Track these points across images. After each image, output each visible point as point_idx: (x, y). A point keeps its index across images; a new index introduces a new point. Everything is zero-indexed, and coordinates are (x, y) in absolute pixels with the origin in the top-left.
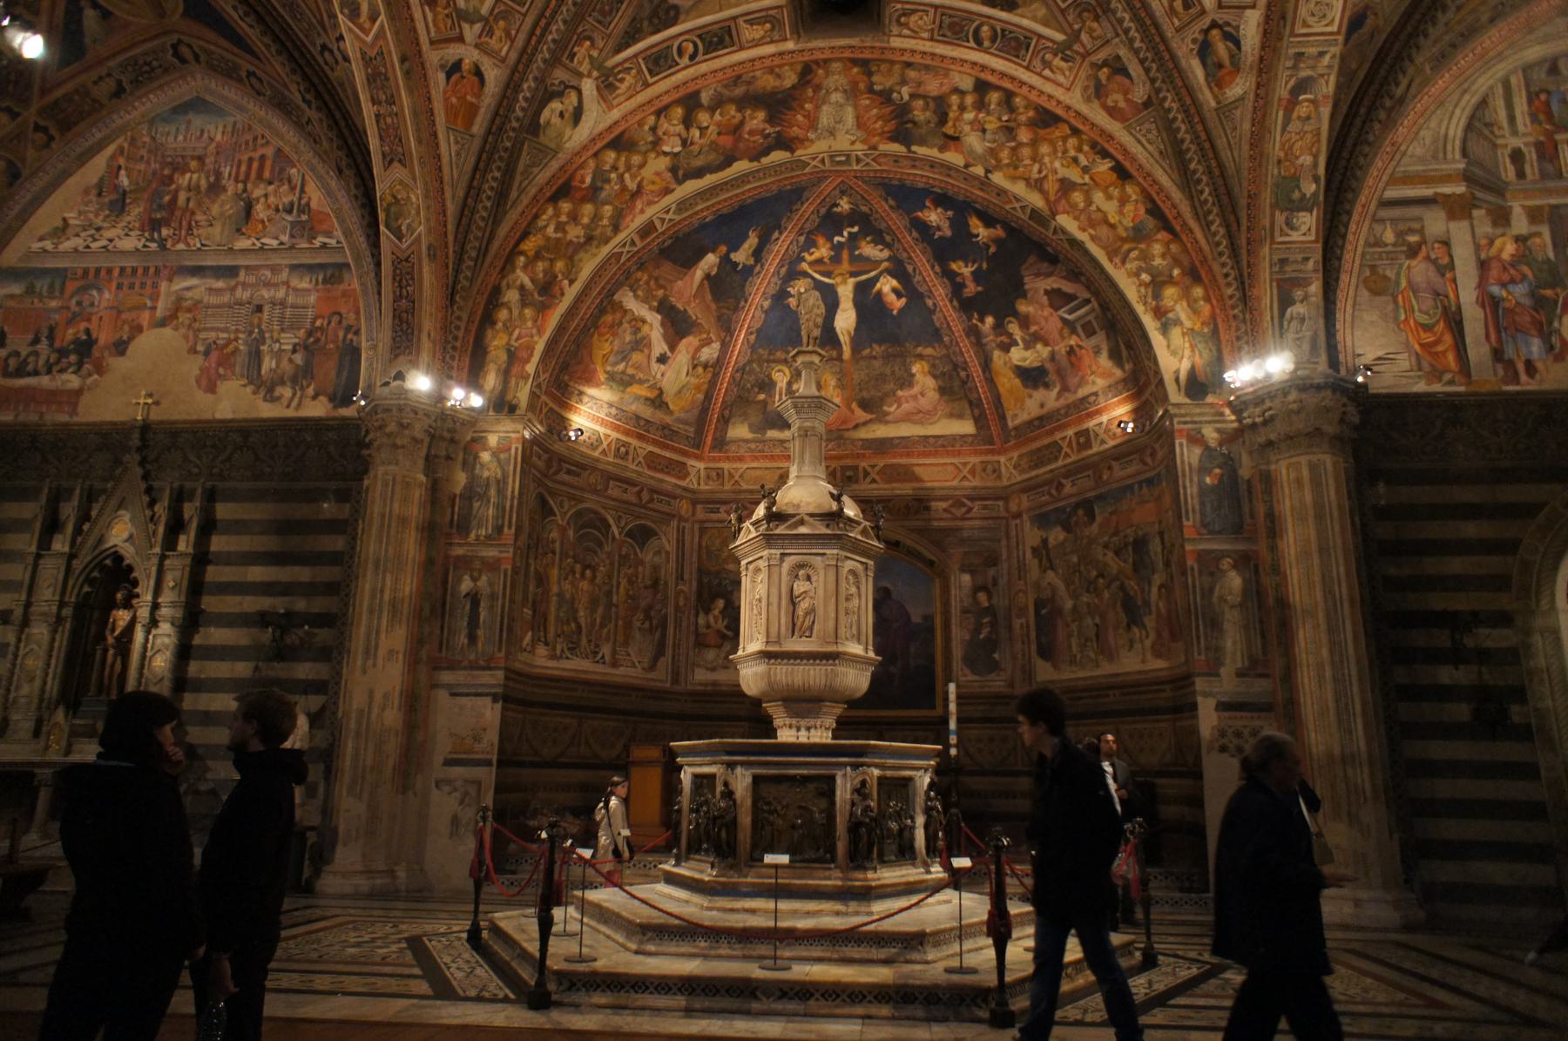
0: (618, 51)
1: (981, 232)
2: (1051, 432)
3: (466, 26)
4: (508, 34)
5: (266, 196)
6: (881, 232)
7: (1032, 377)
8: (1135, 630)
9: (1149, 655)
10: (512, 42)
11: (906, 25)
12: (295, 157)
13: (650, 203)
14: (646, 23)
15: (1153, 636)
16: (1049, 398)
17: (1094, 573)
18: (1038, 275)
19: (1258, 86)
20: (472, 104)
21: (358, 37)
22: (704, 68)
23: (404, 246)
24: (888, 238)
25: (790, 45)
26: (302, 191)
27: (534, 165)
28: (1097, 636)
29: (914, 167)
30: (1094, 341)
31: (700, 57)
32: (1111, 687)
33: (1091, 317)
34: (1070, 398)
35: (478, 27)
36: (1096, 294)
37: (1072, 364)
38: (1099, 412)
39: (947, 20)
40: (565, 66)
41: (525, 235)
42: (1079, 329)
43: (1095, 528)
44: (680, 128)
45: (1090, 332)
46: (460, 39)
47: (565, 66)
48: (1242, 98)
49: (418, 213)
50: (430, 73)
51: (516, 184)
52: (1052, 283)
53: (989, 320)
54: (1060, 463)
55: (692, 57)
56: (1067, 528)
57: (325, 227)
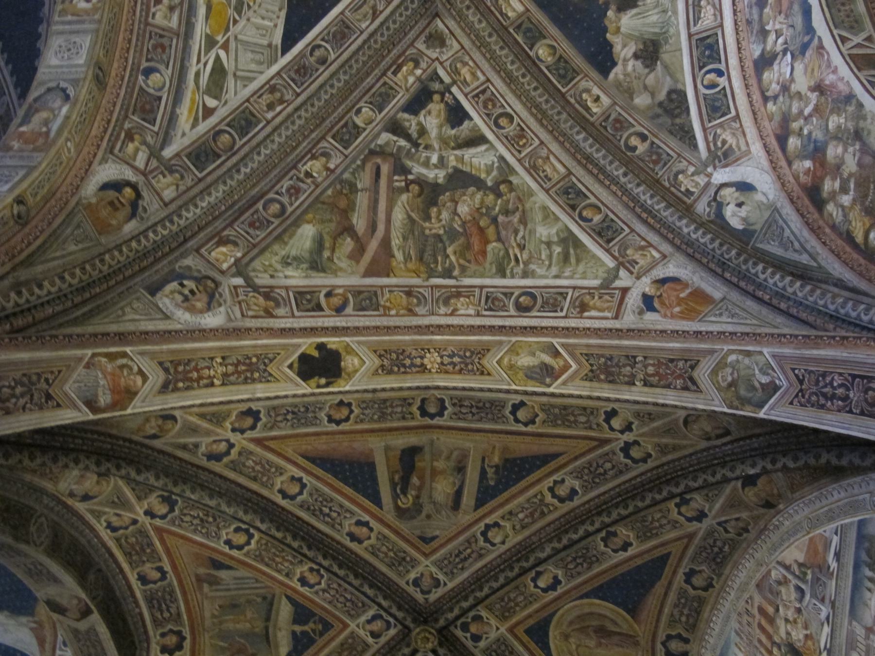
0: (695, 146)
3: (618, 283)
4: (642, 248)
5: (787, 620)
10: (651, 245)
12: (764, 570)
13: (829, 65)
14: (678, 121)
20: (691, 293)
21: (572, 378)
22: (733, 61)
23: (785, 383)
26: (787, 568)
27: (781, 235)
31: (722, 67)
35: (622, 273)
40: (695, 201)
41: (849, 238)
44: (776, 67)
46: (625, 291)
47: (695, 201)
49: (748, 354)
50: (641, 326)
51: (795, 257)
55: (720, 73)
57: (820, 548)
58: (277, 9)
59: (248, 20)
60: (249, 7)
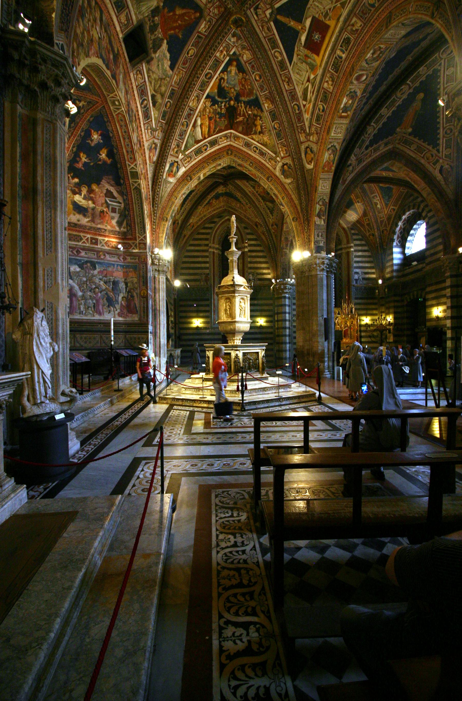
1: (103, 155)
2: (79, 231)
6: (74, 121)
7: (78, 209)
8: (112, 308)
9: (117, 316)
11: (137, 75)
15: (119, 311)
16: (84, 221)
17: (94, 286)
18: (108, 183)
19: (176, 184)
24: (73, 125)
25: (121, 36)
28: (94, 306)
29: (121, 126)
30: (113, 214)
32: (100, 323)
33: (117, 208)
34: (94, 225)
36: (126, 205)
37: (100, 216)
38: (105, 236)
39: (143, 88)
42: (110, 207)
43: (96, 272)
45: (114, 211)
48: (171, 183)
52: (112, 189)
53: (76, 180)
54: (80, 243)
56: (81, 266)
58: (311, 9)
59: (324, 8)
60: (322, 14)
